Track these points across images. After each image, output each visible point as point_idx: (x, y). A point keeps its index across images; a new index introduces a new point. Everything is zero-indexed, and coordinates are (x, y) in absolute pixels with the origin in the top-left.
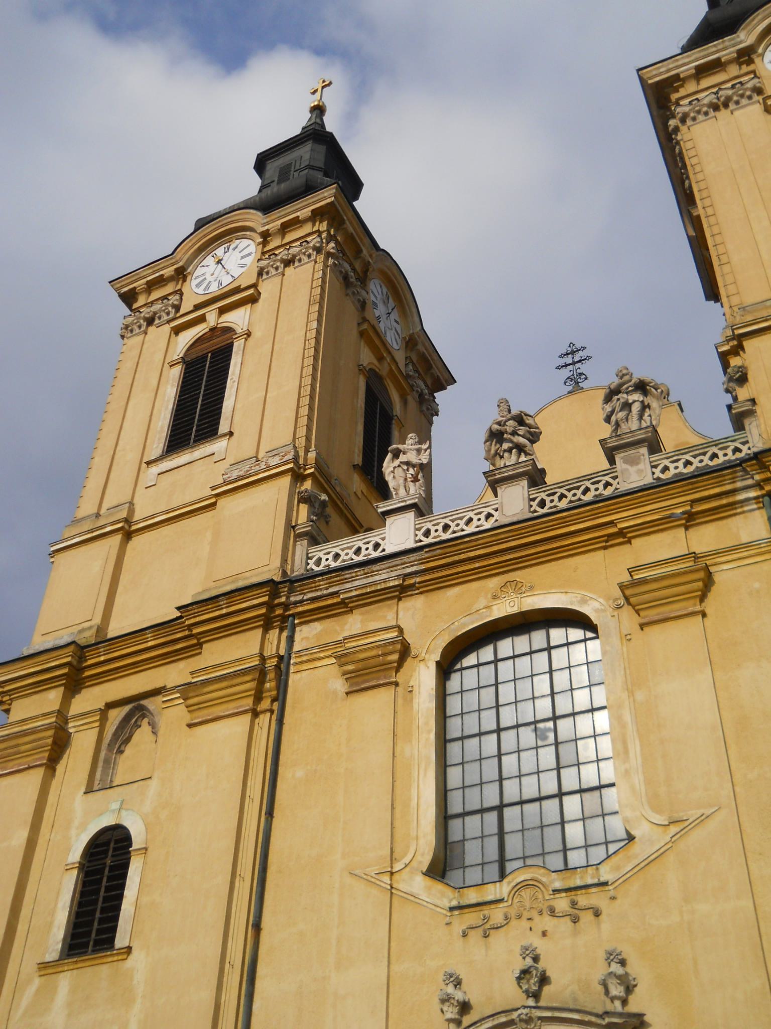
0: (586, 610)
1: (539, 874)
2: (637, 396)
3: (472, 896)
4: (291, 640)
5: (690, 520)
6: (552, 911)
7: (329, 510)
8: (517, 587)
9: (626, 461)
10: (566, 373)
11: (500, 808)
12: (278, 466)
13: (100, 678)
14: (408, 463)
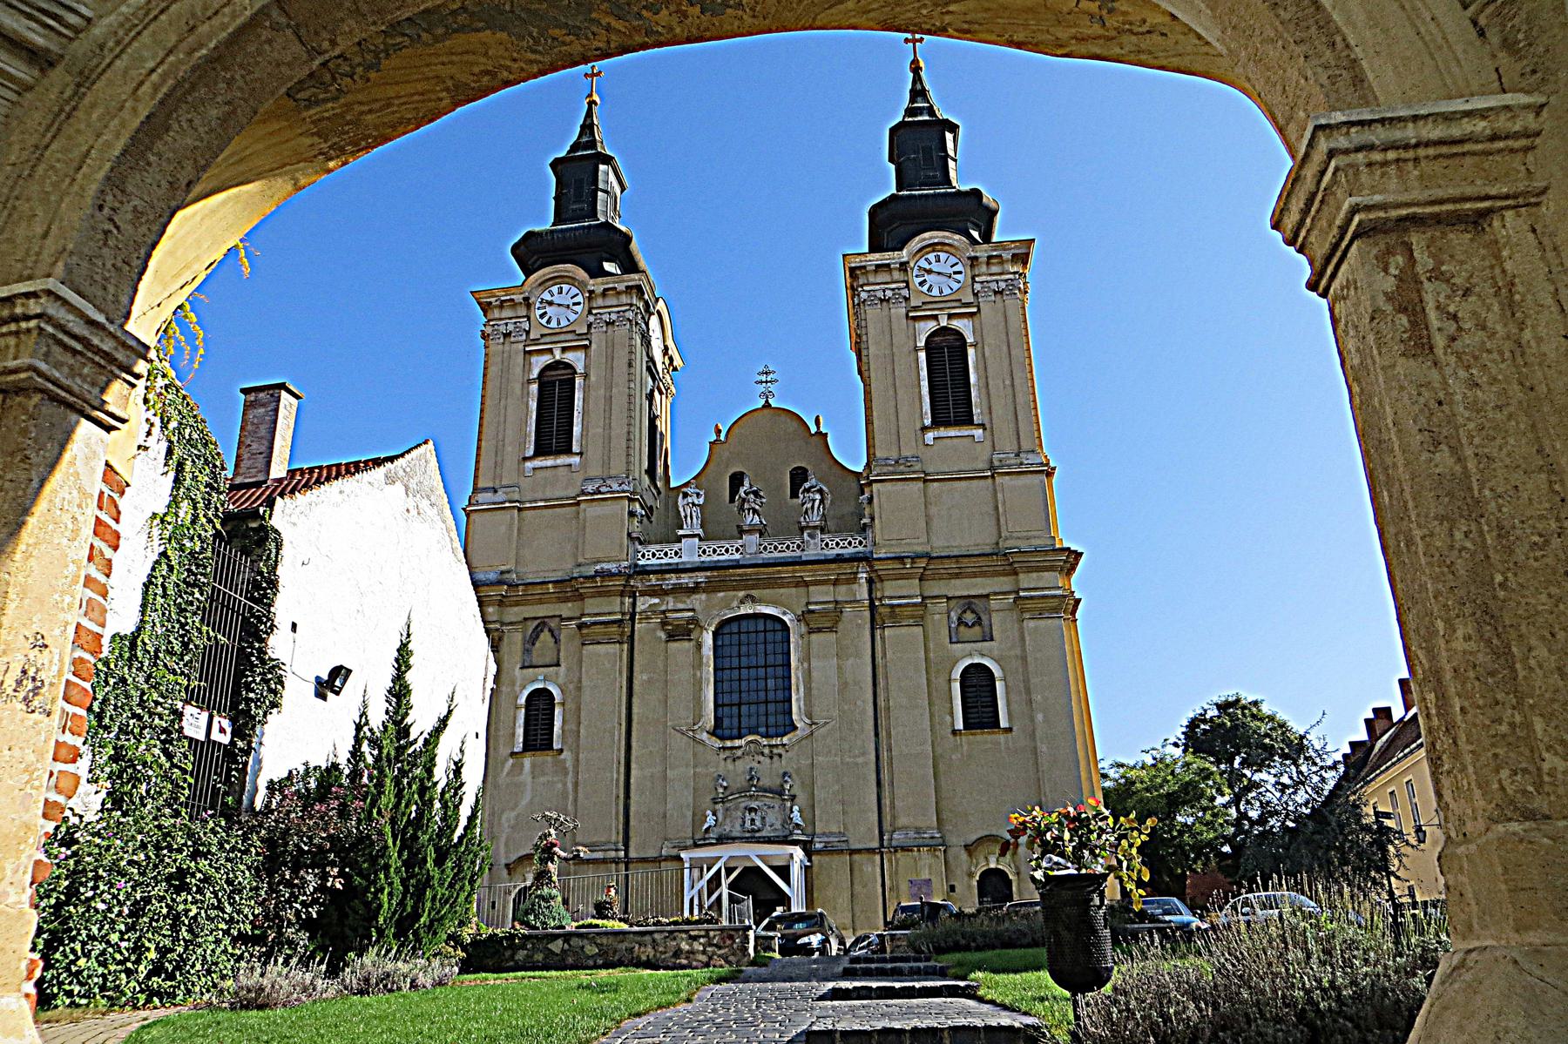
0: (785, 618)
1: (758, 738)
2: (818, 496)
3: (729, 744)
4: (634, 605)
5: (836, 583)
6: (762, 754)
7: (645, 519)
8: (753, 600)
9: (809, 535)
10: (762, 388)
11: (739, 705)
12: (618, 492)
13: (517, 604)
14: (693, 504)
